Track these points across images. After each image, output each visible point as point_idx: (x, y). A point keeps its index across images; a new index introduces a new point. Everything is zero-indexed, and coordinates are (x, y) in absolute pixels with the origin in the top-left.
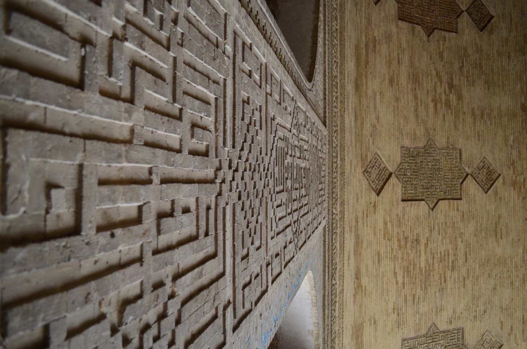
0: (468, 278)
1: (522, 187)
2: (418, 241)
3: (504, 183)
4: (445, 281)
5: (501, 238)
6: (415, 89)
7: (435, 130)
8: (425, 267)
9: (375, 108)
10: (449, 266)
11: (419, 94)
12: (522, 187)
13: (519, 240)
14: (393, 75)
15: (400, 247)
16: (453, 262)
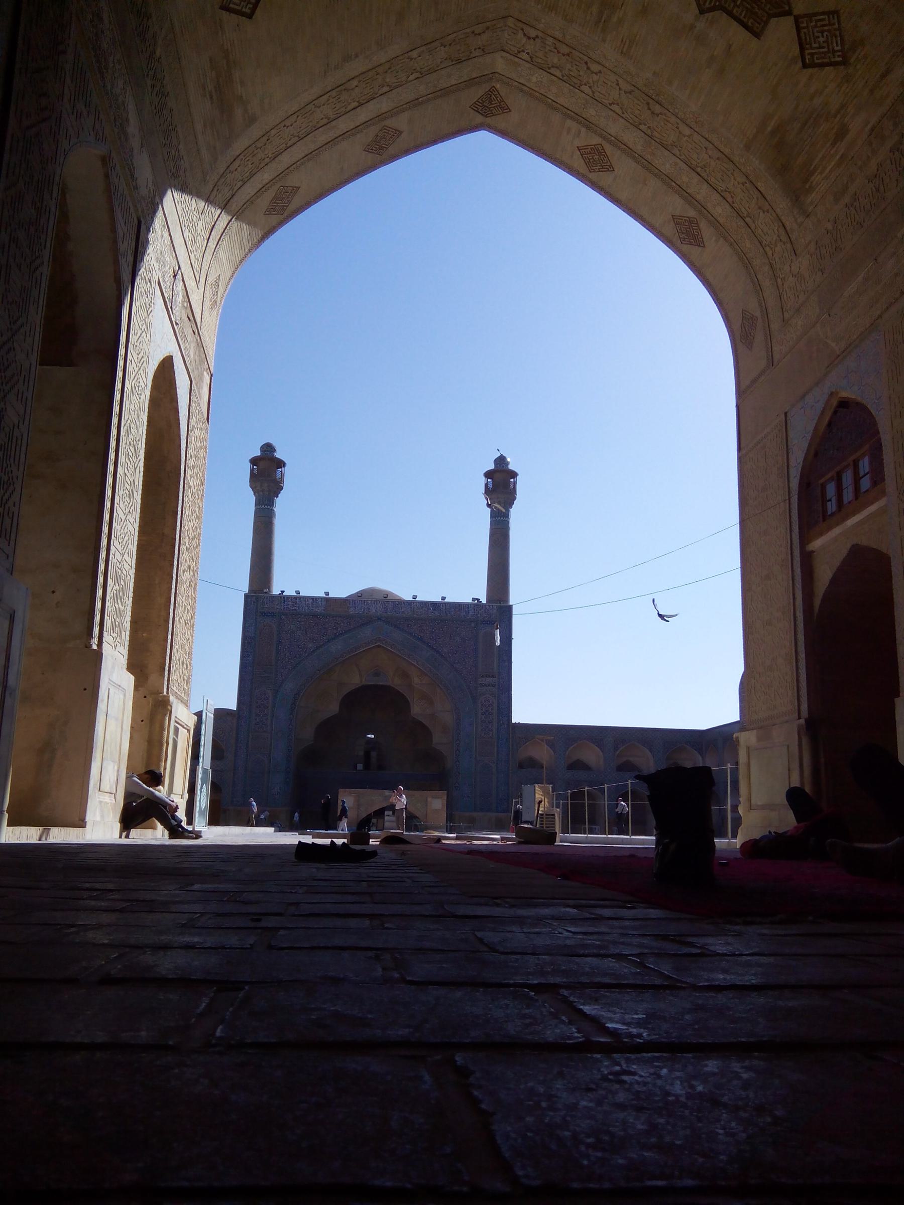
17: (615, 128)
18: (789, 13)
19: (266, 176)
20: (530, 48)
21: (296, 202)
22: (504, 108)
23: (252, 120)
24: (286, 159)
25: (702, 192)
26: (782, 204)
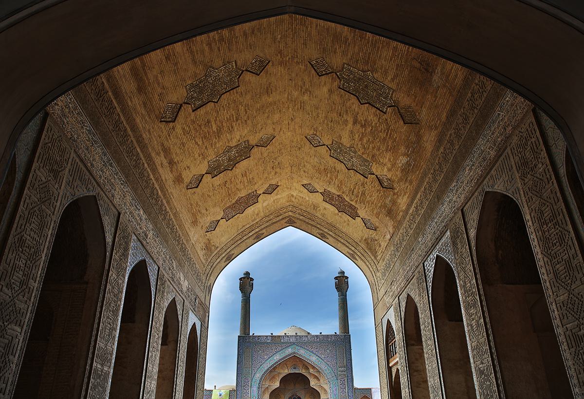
0: (248, 119)
1: (288, 63)
2: (209, 122)
3: (273, 65)
4: (232, 128)
5: (272, 93)
6: (190, 47)
7: (212, 61)
8: (217, 129)
9: (158, 84)
10: (234, 120)
11: (194, 48)
12: (288, 63)
13: (285, 90)
14: (169, 52)
15: (197, 131)
16: (236, 117)
18: (359, 217)
20: (298, 211)
23: (218, 247)
25: (353, 249)
26: (373, 258)
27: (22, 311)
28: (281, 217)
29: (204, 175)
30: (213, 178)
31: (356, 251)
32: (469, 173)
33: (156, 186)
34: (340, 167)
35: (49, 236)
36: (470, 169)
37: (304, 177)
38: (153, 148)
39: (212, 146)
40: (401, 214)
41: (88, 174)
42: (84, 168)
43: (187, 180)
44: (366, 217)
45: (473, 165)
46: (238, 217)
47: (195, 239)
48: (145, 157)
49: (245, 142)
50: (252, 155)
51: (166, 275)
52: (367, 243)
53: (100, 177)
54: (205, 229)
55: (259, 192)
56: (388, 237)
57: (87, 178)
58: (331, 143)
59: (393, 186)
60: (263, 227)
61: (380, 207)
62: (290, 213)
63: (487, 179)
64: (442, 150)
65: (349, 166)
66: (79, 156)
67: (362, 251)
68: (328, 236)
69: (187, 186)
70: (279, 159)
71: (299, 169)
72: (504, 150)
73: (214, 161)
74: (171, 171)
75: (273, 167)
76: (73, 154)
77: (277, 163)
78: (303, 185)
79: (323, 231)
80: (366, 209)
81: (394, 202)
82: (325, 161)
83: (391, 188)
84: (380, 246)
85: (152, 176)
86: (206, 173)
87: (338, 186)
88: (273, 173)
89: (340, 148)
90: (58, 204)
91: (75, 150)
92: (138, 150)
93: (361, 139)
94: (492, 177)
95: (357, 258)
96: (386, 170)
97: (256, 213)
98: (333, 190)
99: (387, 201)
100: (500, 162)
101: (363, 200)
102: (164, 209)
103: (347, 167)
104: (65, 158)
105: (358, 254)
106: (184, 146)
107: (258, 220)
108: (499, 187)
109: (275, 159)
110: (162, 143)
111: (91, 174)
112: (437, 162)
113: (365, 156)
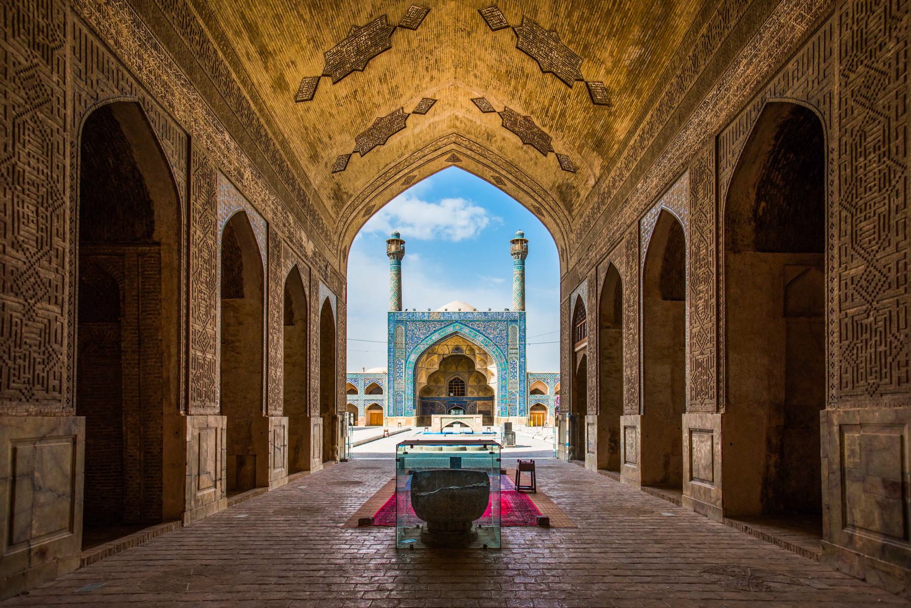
17: (504, 173)
19: (360, 207)
21: (375, 209)
22: (459, 160)
23: (351, 196)
24: (367, 200)
25: (540, 200)
26: (566, 213)
27: (54, 283)
28: (439, 152)
29: (319, 78)
30: (334, 83)
31: (544, 203)
32: (746, 70)
33: (244, 93)
34: (531, 67)
35: (68, 168)
36: (750, 63)
37: (474, 87)
38: (227, 21)
39: (327, 24)
40: (616, 146)
41: (112, 59)
42: (102, 49)
43: (294, 86)
44: (564, 152)
45: (756, 56)
46: (378, 151)
47: (317, 182)
48: (216, 38)
49: (381, 17)
50: (393, 44)
51: (280, 234)
52: (561, 192)
53: (140, 69)
54: (330, 169)
55: (407, 111)
56: (592, 182)
57: (113, 67)
58: (519, 23)
59: (610, 100)
60: (414, 166)
61: (586, 136)
62: (453, 146)
63: (776, 79)
64: (704, 30)
65: (545, 68)
66: (84, 21)
67: (552, 204)
68: (506, 182)
69: (296, 97)
70: (437, 52)
71: (468, 72)
72: (826, 19)
73: (334, 54)
74: (266, 68)
75: (427, 68)
76: (71, 18)
77: (432, 61)
78: (472, 100)
79: (499, 173)
80: (565, 139)
81: (608, 128)
82: (507, 58)
83: (606, 105)
84: (579, 195)
85: (234, 76)
86: (323, 75)
87: (525, 101)
88: (427, 79)
89: (533, 32)
90: (69, 112)
91: (72, 8)
92: (201, 22)
93: (569, 15)
94: (786, 76)
95: (545, 213)
96: (603, 71)
97: (404, 144)
98: (517, 108)
99: (598, 127)
100: (809, 44)
101: (561, 124)
102: (263, 134)
103: (541, 69)
104: (56, 22)
105: (547, 207)
106: (280, 22)
107: (407, 156)
108: (794, 94)
109: (431, 52)
110: (242, 12)
111: (119, 60)
112: (691, 54)
113: (571, 47)
